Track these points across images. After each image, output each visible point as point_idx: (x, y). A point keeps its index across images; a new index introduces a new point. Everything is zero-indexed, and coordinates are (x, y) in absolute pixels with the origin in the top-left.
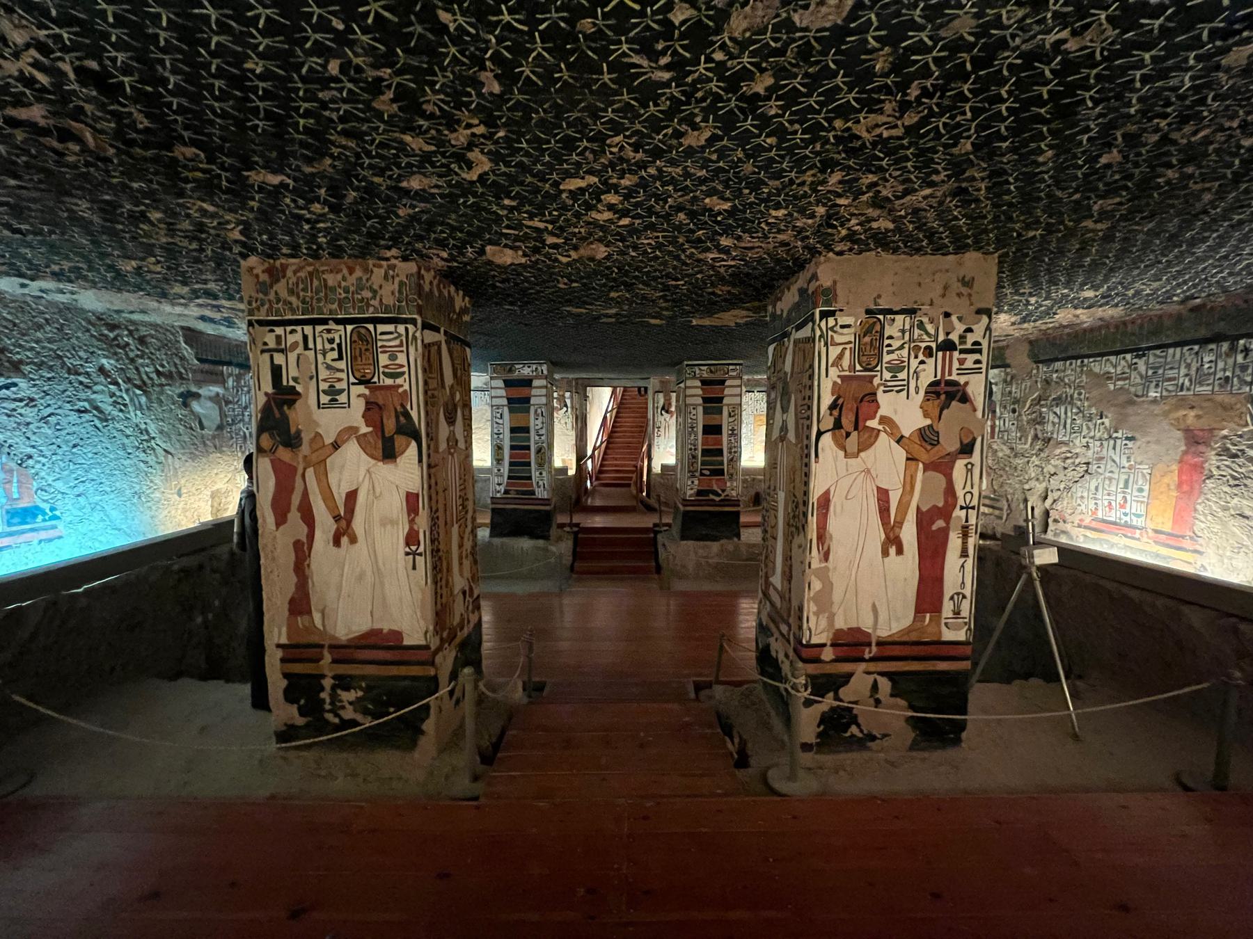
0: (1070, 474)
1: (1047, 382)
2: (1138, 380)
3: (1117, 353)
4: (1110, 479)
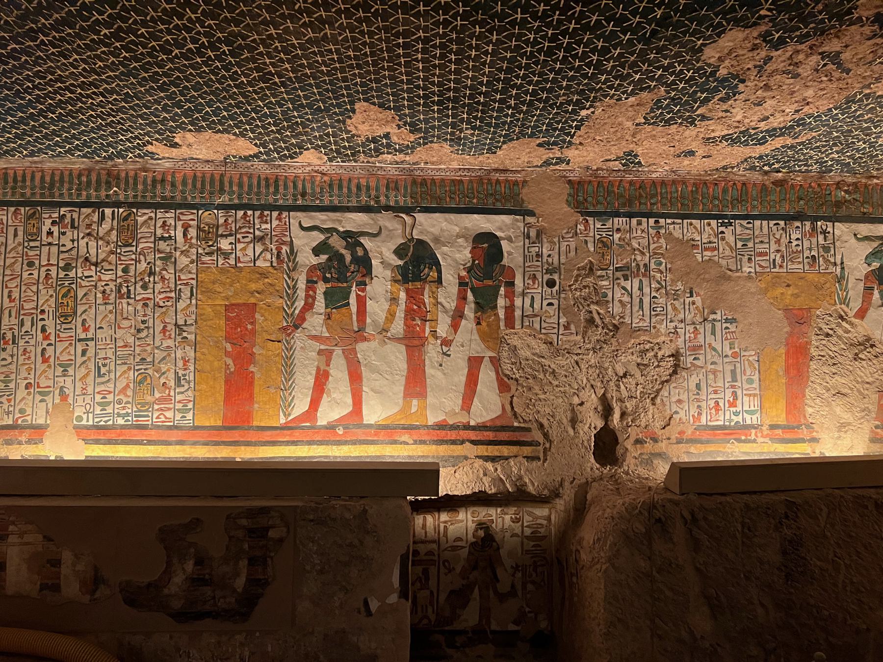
0: (652, 372)
1: (604, 245)
2: (728, 252)
3: (701, 217)
4: (714, 372)
